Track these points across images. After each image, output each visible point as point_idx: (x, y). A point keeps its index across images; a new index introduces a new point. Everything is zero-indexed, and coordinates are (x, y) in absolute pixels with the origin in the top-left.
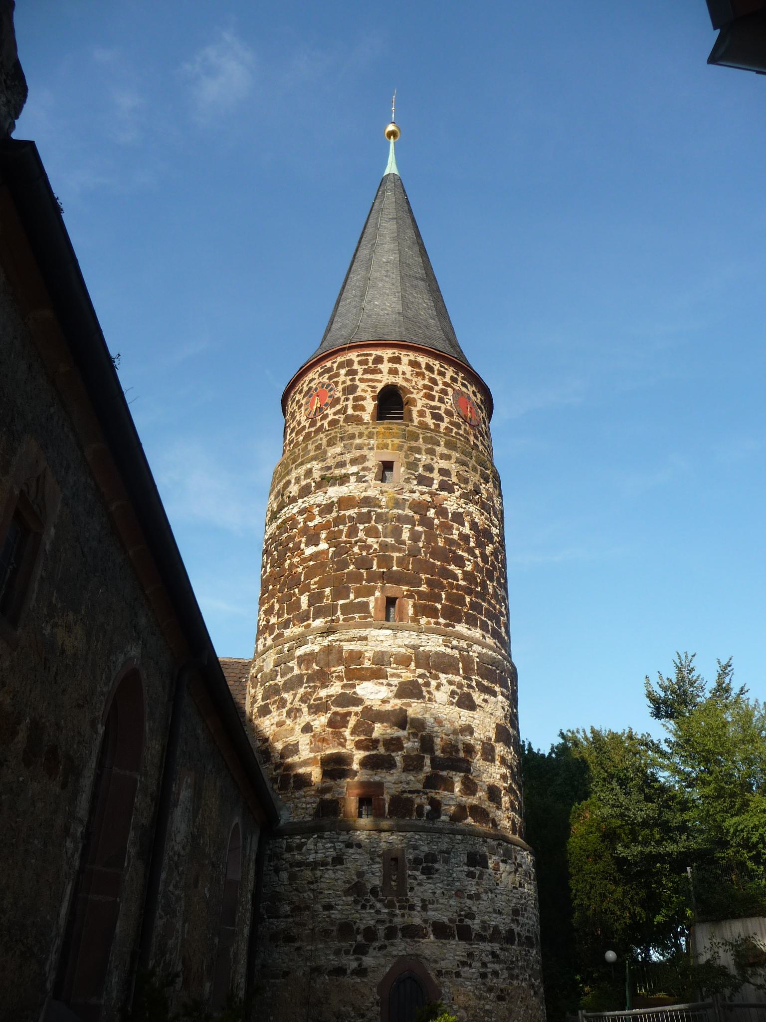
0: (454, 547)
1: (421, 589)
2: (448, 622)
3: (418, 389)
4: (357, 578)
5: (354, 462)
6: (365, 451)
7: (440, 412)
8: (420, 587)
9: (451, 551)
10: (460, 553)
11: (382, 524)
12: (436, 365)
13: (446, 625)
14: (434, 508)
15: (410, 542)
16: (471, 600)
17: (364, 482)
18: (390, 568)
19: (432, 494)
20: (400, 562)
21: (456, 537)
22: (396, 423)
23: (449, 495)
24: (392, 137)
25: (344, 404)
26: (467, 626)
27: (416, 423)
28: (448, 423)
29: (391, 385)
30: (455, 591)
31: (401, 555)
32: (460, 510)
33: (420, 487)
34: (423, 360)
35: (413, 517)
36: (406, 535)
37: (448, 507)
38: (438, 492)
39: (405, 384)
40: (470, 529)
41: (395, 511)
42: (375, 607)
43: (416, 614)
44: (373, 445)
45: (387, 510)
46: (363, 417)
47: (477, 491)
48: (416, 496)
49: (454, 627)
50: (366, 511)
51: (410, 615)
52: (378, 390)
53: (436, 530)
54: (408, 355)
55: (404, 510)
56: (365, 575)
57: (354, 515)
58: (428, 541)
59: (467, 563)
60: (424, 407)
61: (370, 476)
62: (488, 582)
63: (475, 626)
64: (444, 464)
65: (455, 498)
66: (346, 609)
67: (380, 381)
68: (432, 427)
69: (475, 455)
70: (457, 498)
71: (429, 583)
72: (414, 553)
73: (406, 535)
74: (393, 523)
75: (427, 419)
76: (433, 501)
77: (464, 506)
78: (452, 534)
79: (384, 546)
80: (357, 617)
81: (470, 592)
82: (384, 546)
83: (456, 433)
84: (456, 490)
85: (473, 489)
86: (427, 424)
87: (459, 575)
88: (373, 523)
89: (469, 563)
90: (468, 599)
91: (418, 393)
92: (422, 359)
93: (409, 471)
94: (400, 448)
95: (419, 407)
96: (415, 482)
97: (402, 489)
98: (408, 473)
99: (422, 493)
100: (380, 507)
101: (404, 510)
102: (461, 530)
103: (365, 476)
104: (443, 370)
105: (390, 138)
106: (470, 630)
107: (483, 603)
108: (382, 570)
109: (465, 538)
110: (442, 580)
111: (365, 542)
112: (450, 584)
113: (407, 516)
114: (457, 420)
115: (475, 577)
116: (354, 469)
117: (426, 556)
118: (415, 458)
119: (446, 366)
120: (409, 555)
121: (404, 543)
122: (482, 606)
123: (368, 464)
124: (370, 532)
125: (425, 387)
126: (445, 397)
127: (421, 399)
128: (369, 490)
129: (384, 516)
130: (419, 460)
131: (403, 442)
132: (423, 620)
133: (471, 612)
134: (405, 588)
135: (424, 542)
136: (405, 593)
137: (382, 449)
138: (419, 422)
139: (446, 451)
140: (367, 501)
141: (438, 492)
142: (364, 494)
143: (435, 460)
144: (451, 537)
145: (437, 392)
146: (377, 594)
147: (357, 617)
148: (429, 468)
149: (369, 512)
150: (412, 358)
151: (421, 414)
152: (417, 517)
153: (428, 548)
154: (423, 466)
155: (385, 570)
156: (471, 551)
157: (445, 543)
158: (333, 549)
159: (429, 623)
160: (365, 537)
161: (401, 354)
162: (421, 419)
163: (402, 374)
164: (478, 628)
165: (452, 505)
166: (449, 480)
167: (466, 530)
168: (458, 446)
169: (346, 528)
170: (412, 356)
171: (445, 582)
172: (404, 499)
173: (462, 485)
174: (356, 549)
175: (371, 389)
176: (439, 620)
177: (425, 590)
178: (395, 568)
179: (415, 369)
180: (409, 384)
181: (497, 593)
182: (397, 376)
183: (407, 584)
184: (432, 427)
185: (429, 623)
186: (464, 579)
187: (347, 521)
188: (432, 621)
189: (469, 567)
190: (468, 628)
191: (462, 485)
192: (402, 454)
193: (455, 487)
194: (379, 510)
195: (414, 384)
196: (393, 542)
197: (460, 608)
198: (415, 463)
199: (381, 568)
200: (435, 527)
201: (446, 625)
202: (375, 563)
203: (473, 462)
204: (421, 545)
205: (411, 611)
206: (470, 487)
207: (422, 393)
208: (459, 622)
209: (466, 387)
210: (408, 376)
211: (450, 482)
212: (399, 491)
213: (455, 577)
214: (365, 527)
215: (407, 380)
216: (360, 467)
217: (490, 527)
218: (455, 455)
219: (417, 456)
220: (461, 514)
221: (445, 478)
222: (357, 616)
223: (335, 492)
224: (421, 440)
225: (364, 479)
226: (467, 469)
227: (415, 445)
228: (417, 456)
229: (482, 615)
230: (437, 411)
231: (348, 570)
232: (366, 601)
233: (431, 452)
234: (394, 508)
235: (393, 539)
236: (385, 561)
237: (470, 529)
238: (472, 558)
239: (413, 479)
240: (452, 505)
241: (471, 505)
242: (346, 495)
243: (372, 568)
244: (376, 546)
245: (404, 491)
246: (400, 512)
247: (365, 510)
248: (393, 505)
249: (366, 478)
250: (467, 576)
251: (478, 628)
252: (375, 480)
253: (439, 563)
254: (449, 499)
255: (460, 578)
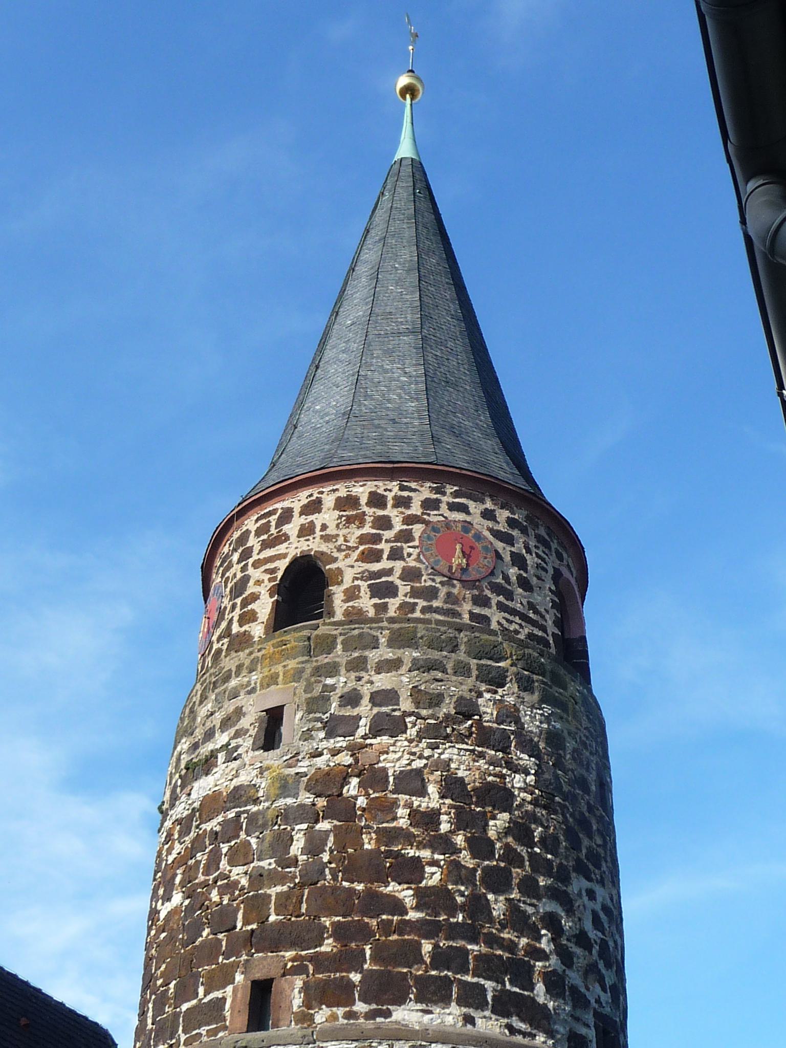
0: (397, 845)
1: (323, 949)
2: (374, 1006)
3: (349, 548)
4: (212, 949)
5: (226, 723)
6: (242, 700)
7: (390, 579)
8: (320, 945)
9: (389, 854)
10: (411, 852)
11: (257, 833)
12: (391, 489)
13: (371, 1015)
14: (358, 776)
15: (305, 857)
16: (436, 946)
17: (235, 759)
18: (263, 921)
19: (354, 749)
20: (283, 902)
21: (403, 823)
22: (295, 630)
23: (392, 741)
24: (408, 96)
25: (230, 617)
26: (419, 1006)
27: (339, 616)
28: (405, 595)
29: (301, 557)
30: (395, 937)
31: (285, 888)
32: (418, 764)
33: (332, 741)
34: (362, 490)
35: (314, 805)
36: (297, 847)
37: (388, 765)
38: (368, 741)
39: (324, 548)
40: (442, 797)
41: (281, 802)
42: (232, 1007)
43: (307, 1004)
44: (255, 683)
45: (267, 804)
46: (252, 633)
47: (467, 710)
48: (320, 762)
49: (388, 1014)
50: (233, 815)
51: (295, 1009)
52: (280, 574)
53: (360, 820)
54: (334, 491)
55: (296, 796)
56: (224, 943)
57: (218, 828)
58: (341, 846)
59: (428, 869)
60: (357, 579)
61: (246, 743)
62: (490, 897)
63: (444, 1000)
64: (383, 681)
65: (406, 743)
66: (195, 1018)
67: (284, 556)
68: (371, 613)
69: (465, 640)
70: (410, 741)
71: (339, 932)
72: (311, 877)
73: (297, 847)
74: (276, 827)
75: (361, 601)
76: (357, 761)
77: (427, 753)
78: (395, 819)
79: (258, 878)
80: (204, 1033)
81: (429, 929)
82: (258, 878)
83: (424, 610)
84: (409, 725)
85: (453, 712)
86: (360, 612)
87: (407, 900)
88: (243, 835)
89: (434, 869)
90: (427, 947)
91: (347, 556)
92: (361, 489)
93: (311, 716)
94: (297, 675)
95: (347, 582)
96: (322, 734)
97: (298, 754)
98: (309, 721)
99: (335, 752)
100: (256, 801)
101: (296, 796)
102: (416, 804)
103: (237, 748)
104: (405, 494)
105: (404, 98)
106: (430, 1012)
107: (469, 947)
108: (249, 928)
109: (429, 819)
110: (366, 920)
111: (228, 877)
112: (386, 928)
113: (302, 806)
114: (429, 583)
115: (449, 895)
116: (222, 739)
117: (335, 878)
118: (325, 686)
119: (413, 485)
120: (302, 885)
121: (295, 862)
122: (466, 952)
123: (245, 723)
124: (240, 855)
125: (362, 539)
126: (405, 546)
127: (352, 567)
128: (242, 772)
129: (261, 817)
130: (333, 688)
131: (303, 662)
132: (321, 1016)
133: (433, 973)
134: (289, 954)
135: (331, 851)
136: (290, 965)
137: (268, 686)
138: (347, 613)
139: (390, 654)
140: (240, 795)
141: (368, 741)
142: (236, 782)
143: (366, 678)
144: (394, 824)
145: (387, 541)
146: (239, 978)
147: (204, 1033)
148: (351, 699)
149: (238, 815)
150: (343, 493)
151: (352, 594)
152: (321, 802)
153: (340, 860)
154: (341, 697)
155: (254, 926)
156: (444, 844)
157: (378, 841)
158: (187, 902)
159: (334, 1017)
160: (229, 868)
161: (322, 493)
162: (350, 604)
163: (321, 530)
164: (453, 1004)
165: (399, 759)
166: (394, 710)
167: (432, 799)
168: (419, 635)
169: (205, 857)
170: (343, 489)
171: (374, 922)
172: (297, 774)
173: (424, 712)
174: (215, 896)
175: (269, 576)
176: (355, 1008)
177: (329, 949)
178: (273, 918)
179: (344, 513)
180: (331, 545)
181: (525, 912)
182: (311, 538)
183: (292, 945)
184: (371, 613)
185: (334, 1017)
186: (417, 908)
187: (207, 843)
188: (340, 1011)
189: (433, 877)
190: (423, 1011)
191: (424, 712)
192: (301, 686)
193: (408, 720)
194: (254, 809)
195: (341, 540)
196: (273, 866)
197: (405, 970)
198: (323, 696)
199: (249, 925)
200: (359, 813)
201: (371, 1015)
202: (240, 916)
203: (462, 655)
204: (326, 857)
205: (297, 1001)
206: (447, 708)
207: (355, 555)
208: (400, 1000)
209: (464, 509)
210: (332, 530)
211: (397, 713)
212: (290, 761)
213: (398, 907)
214: (231, 847)
215: (327, 538)
216: (232, 731)
217: (502, 777)
218: (409, 655)
219: (329, 681)
220: (419, 772)
221: (384, 709)
222: (203, 1030)
223: (203, 787)
224: (339, 647)
225: (235, 754)
226: (440, 675)
227: (326, 661)
228: (329, 681)
229: (466, 971)
230: (384, 579)
231: (200, 939)
232: (220, 996)
233: (358, 665)
234: (278, 797)
235: (272, 861)
236: (257, 906)
237: (442, 797)
238: (442, 857)
239: (318, 729)
240: (399, 759)
241: (448, 745)
242: (210, 793)
243: (235, 927)
244: (244, 882)
245: (300, 757)
246: (290, 801)
247: (231, 814)
248: (277, 792)
249: (240, 751)
250: (425, 898)
251: (453, 1004)
252: (252, 750)
253: (360, 887)
254: (391, 748)
255: (408, 906)
